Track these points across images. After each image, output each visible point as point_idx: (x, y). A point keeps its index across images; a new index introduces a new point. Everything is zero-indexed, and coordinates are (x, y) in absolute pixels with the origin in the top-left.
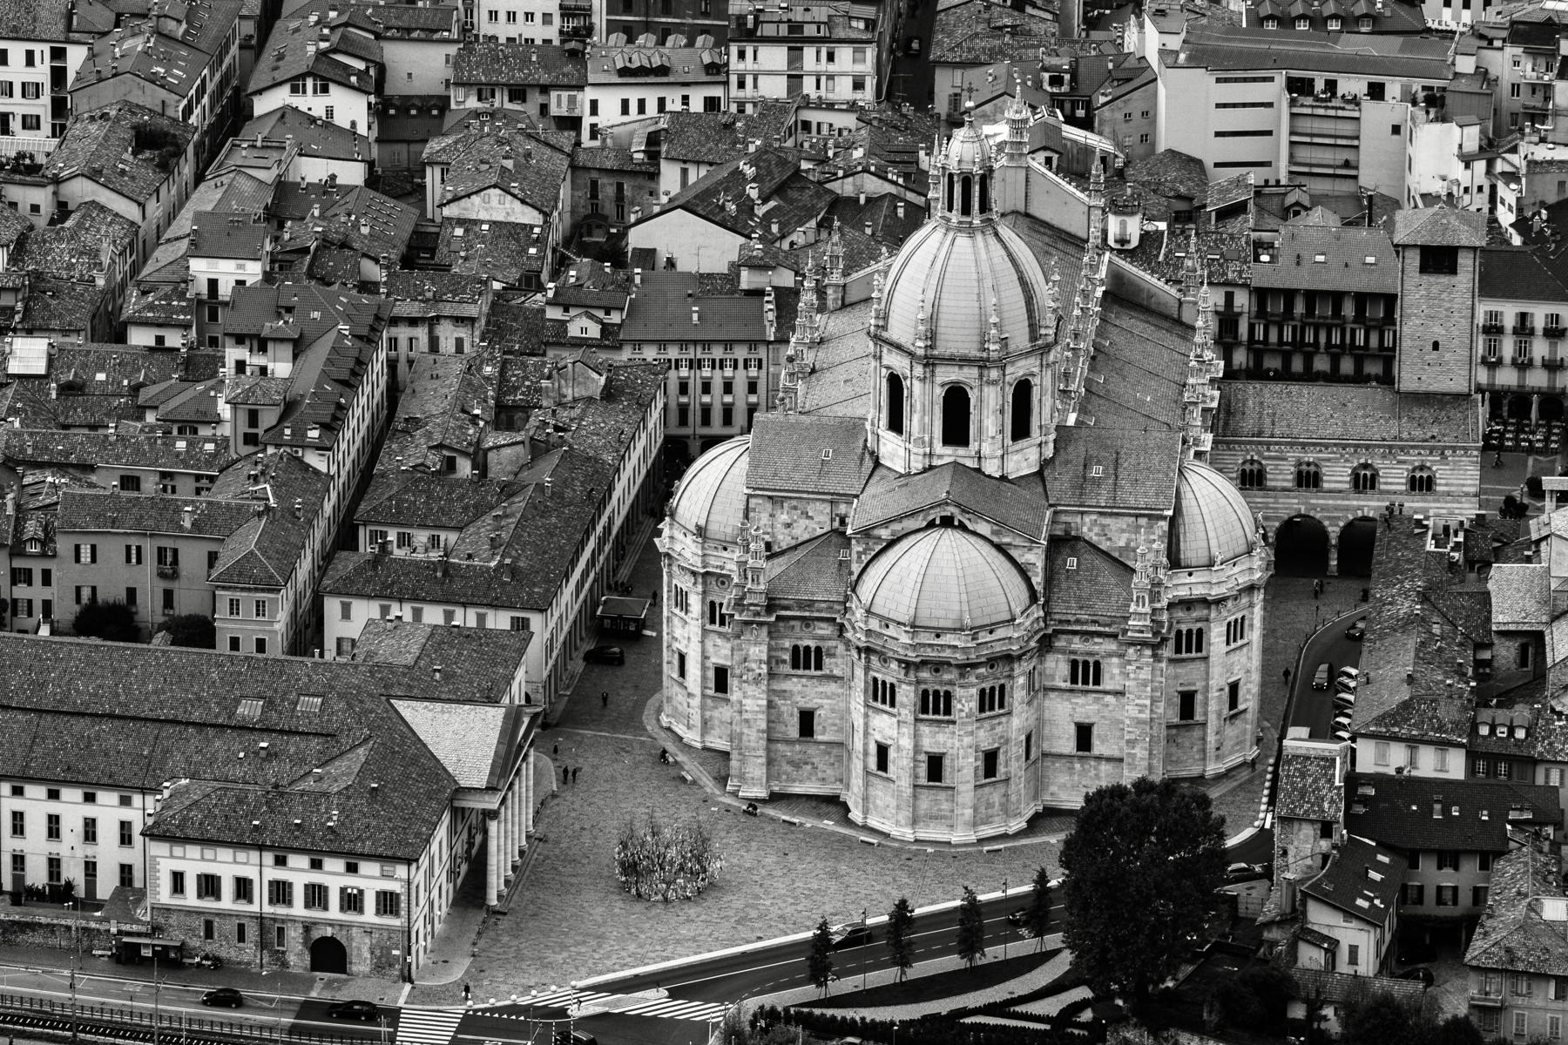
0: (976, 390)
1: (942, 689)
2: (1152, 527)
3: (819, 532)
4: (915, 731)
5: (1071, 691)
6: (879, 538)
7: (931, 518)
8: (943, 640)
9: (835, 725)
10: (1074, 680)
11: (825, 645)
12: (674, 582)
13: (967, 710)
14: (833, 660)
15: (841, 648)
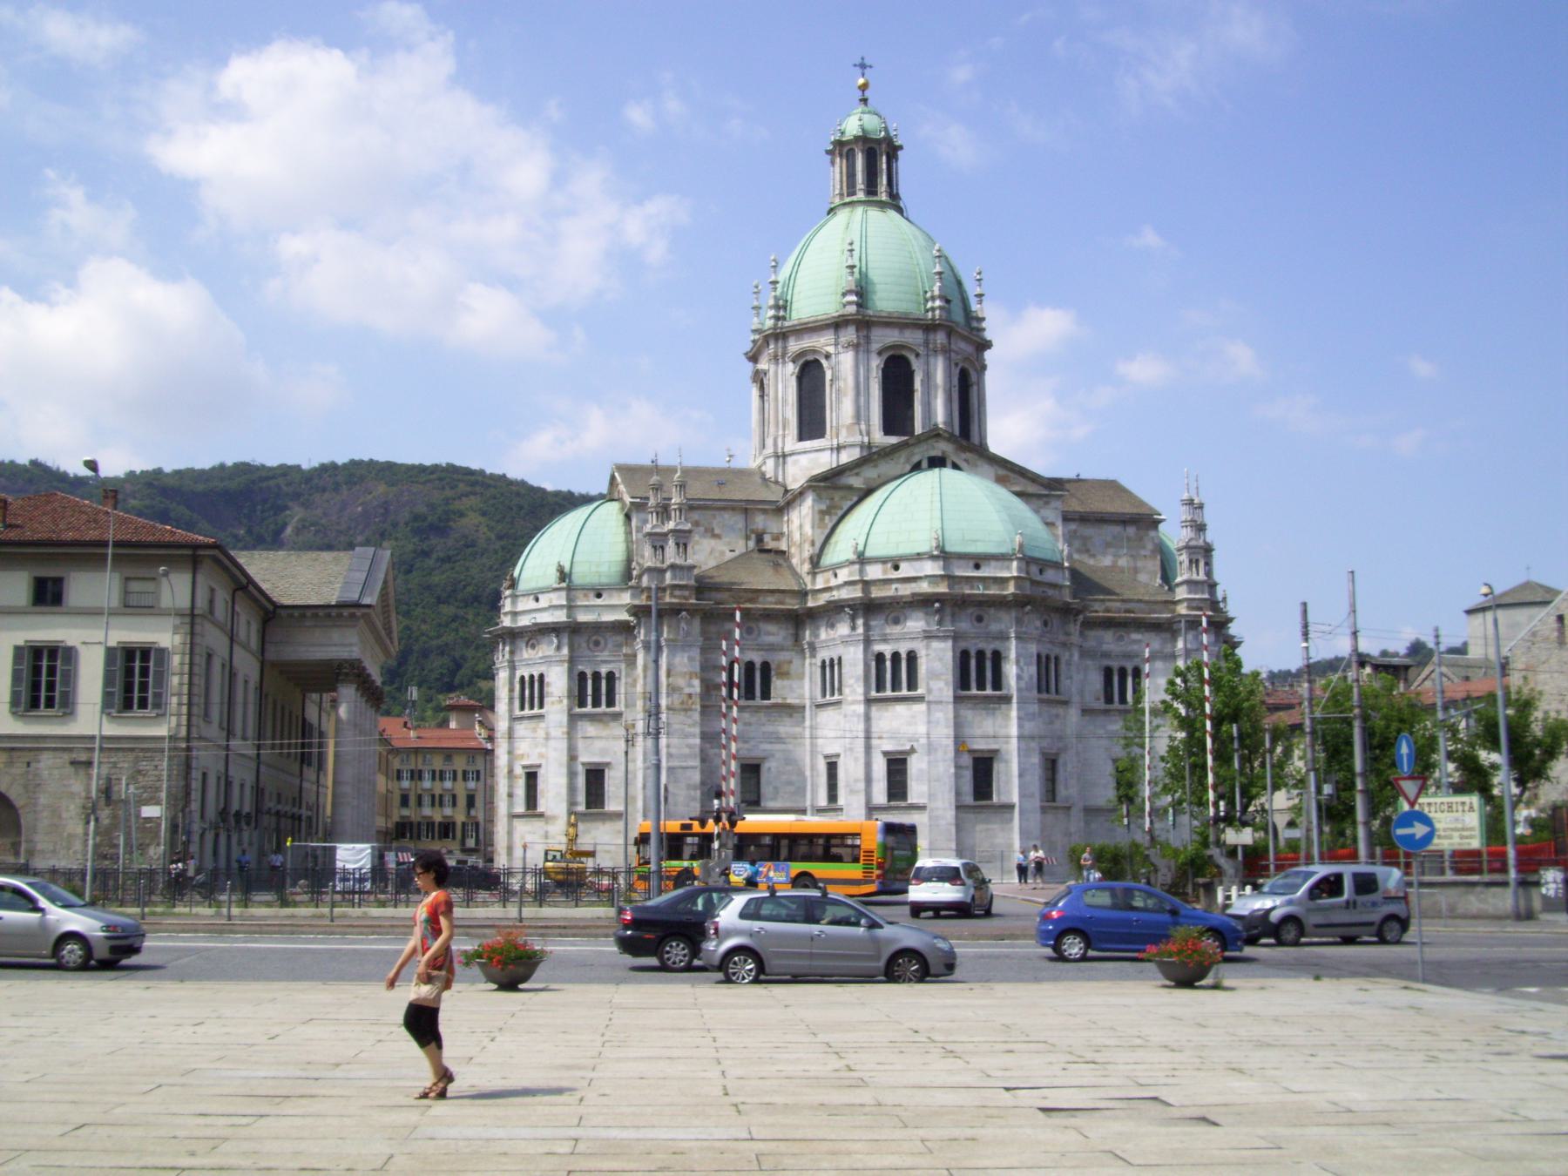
0: (922, 360)
1: (989, 648)
2: (1141, 539)
3: (729, 555)
4: (956, 716)
5: (1106, 712)
6: (850, 488)
7: (916, 459)
8: (985, 572)
9: (790, 783)
10: (1109, 699)
11: (775, 658)
12: (518, 674)
13: (1026, 676)
14: (786, 682)
15: (796, 662)
